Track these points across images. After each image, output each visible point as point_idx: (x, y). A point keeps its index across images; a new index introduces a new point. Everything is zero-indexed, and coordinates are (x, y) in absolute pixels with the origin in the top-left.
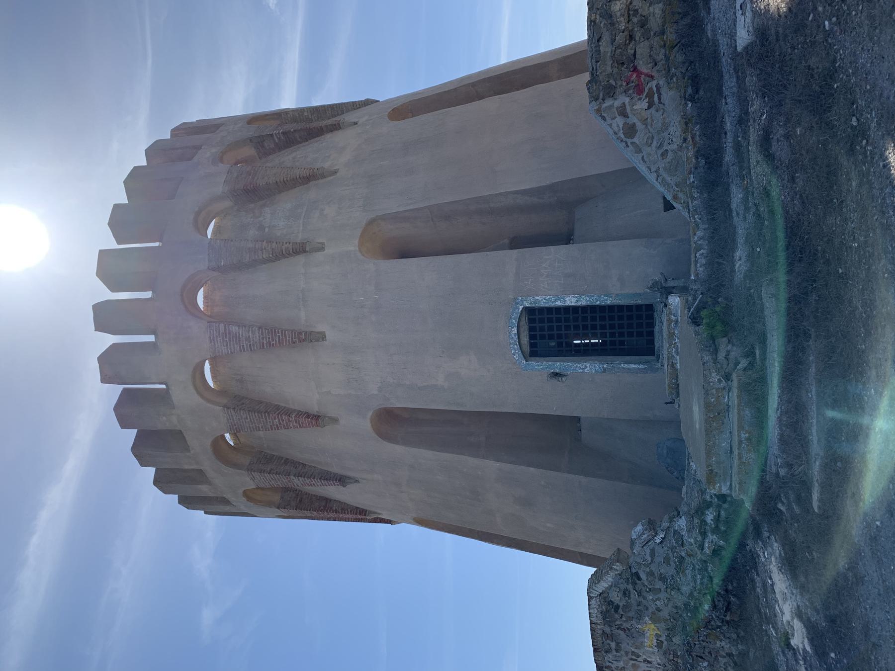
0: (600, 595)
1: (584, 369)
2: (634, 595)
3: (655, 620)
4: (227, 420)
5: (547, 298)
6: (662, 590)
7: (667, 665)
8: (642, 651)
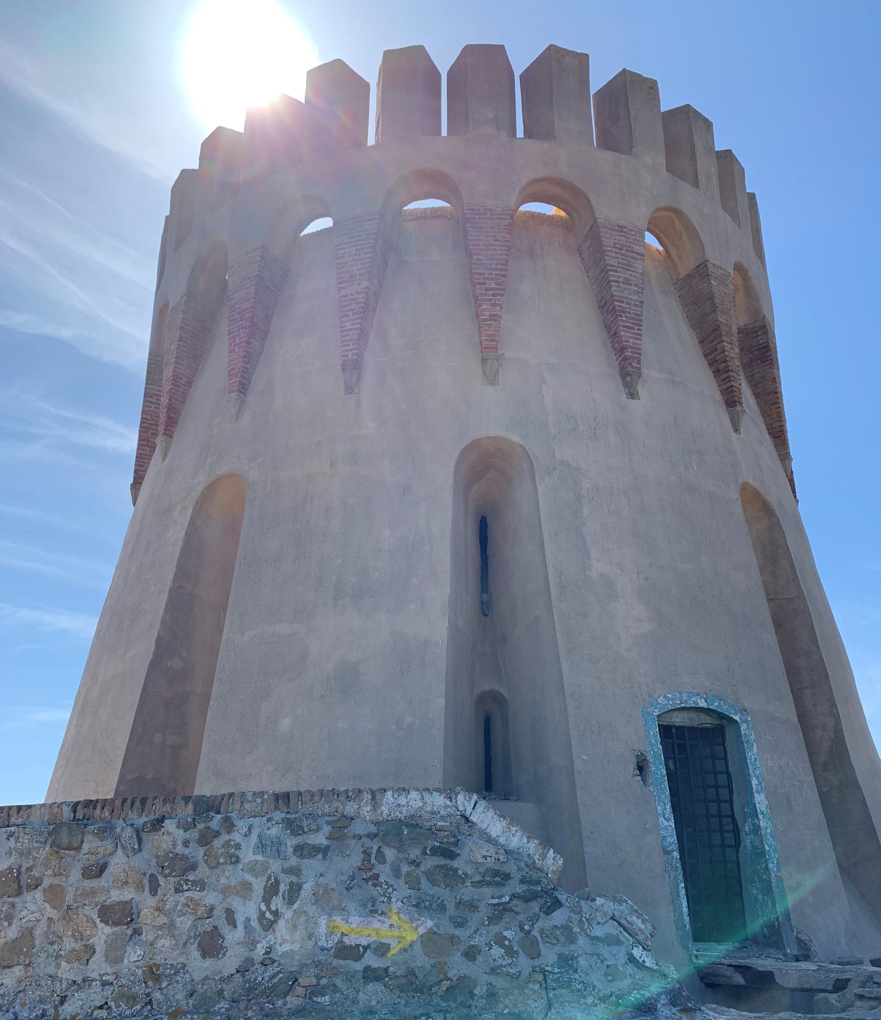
0: (463, 816)
1: (664, 816)
2: (489, 896)
3: (429, 939)
4: (491, 210)
5: (758, 764)
6: (537, 962)
7: (270, 971)
8: (311, 909)
